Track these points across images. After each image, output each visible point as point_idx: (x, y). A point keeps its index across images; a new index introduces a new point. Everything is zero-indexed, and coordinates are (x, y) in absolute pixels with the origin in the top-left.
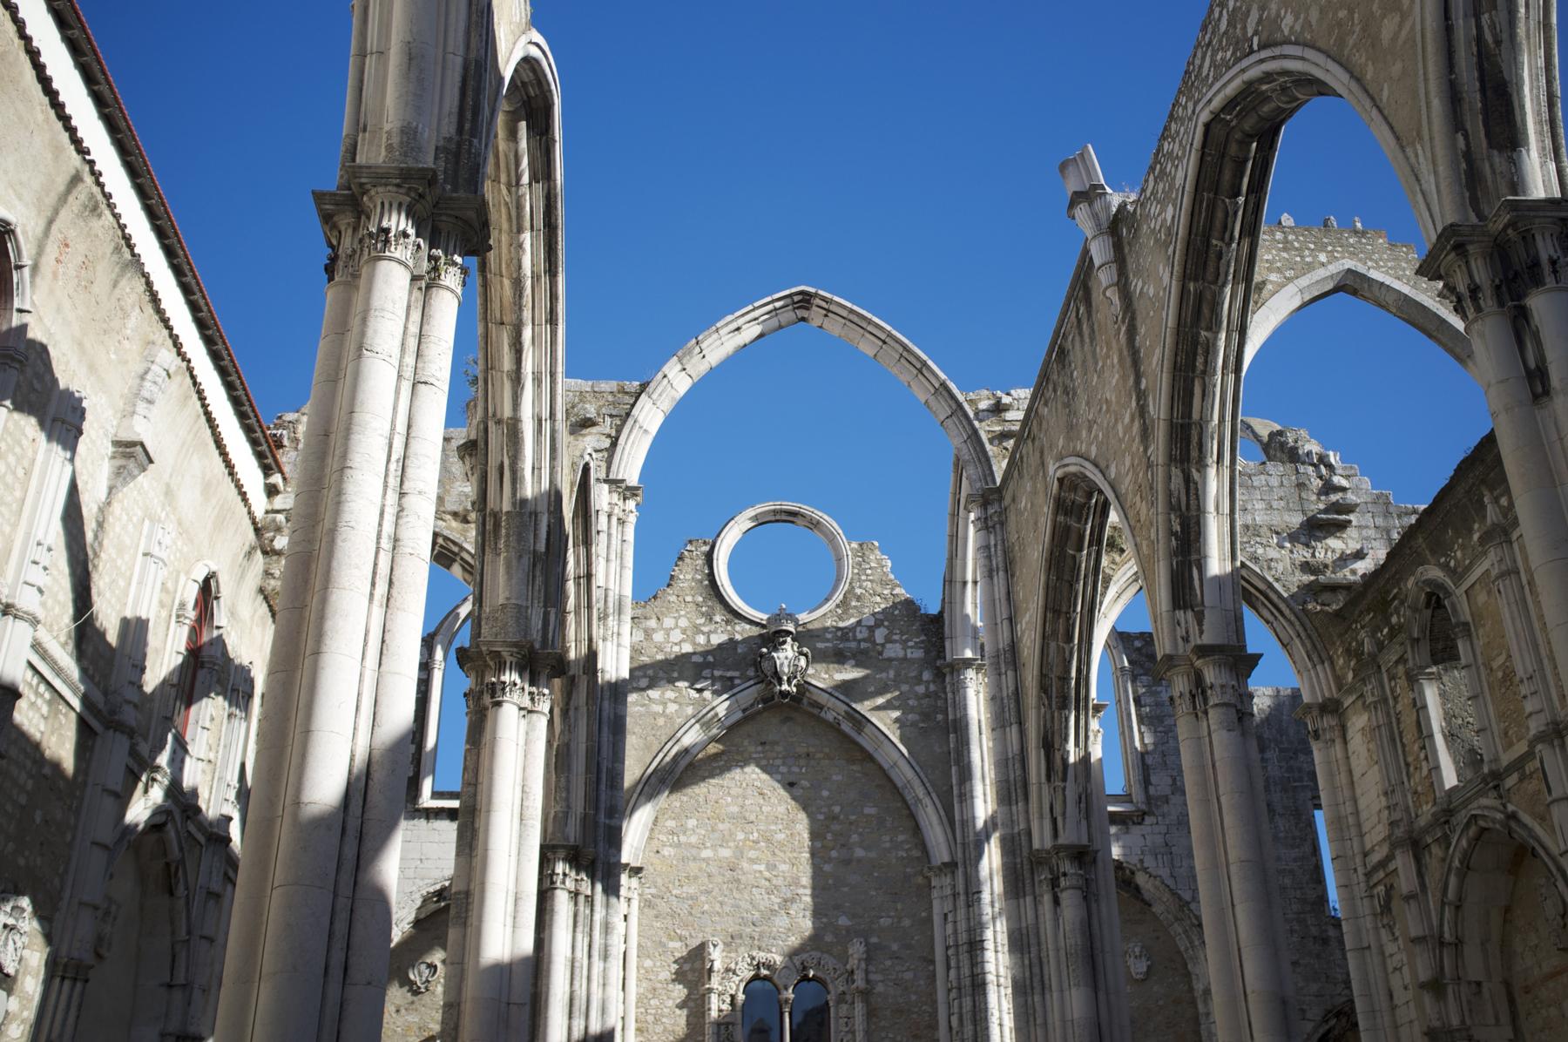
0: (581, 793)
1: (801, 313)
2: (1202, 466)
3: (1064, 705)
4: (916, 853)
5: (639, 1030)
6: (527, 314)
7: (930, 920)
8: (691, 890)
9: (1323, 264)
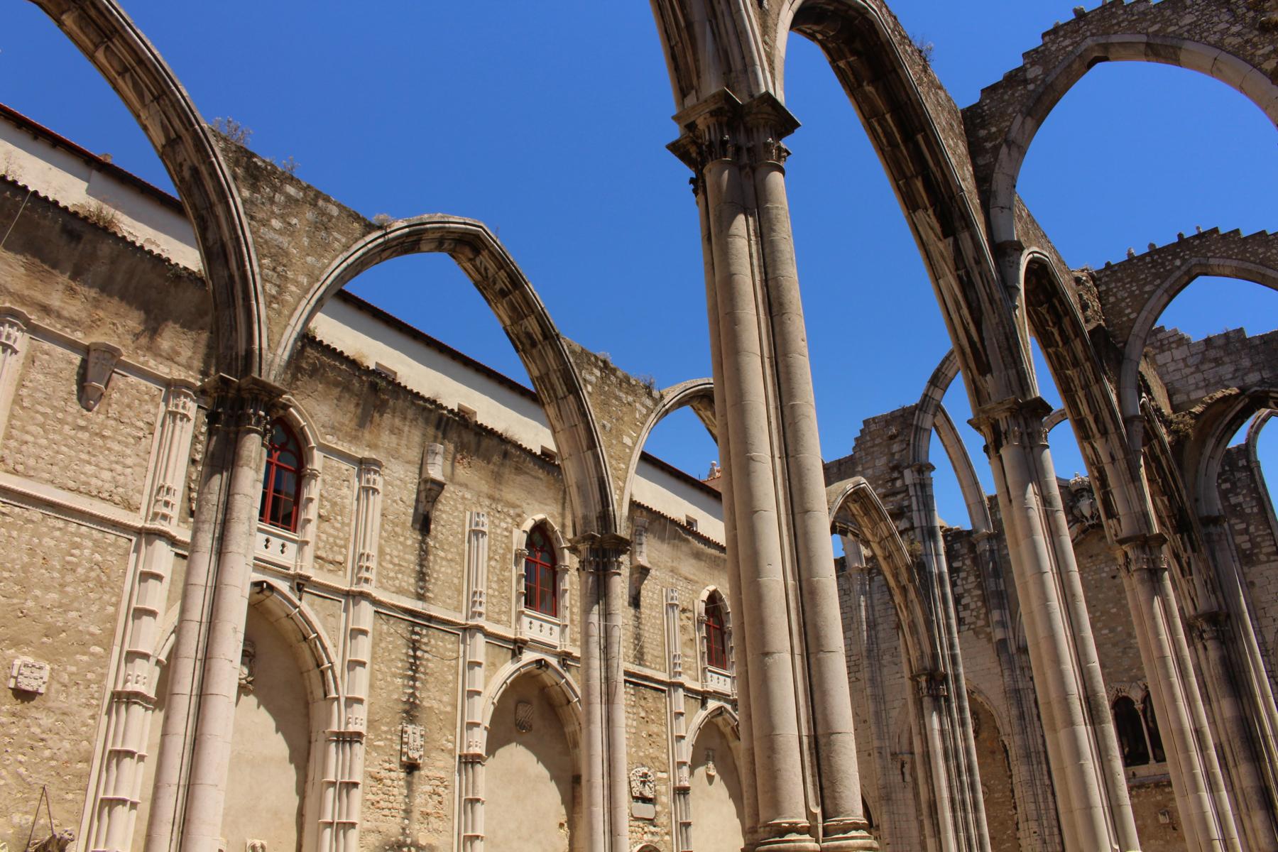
9: (1179, 268)
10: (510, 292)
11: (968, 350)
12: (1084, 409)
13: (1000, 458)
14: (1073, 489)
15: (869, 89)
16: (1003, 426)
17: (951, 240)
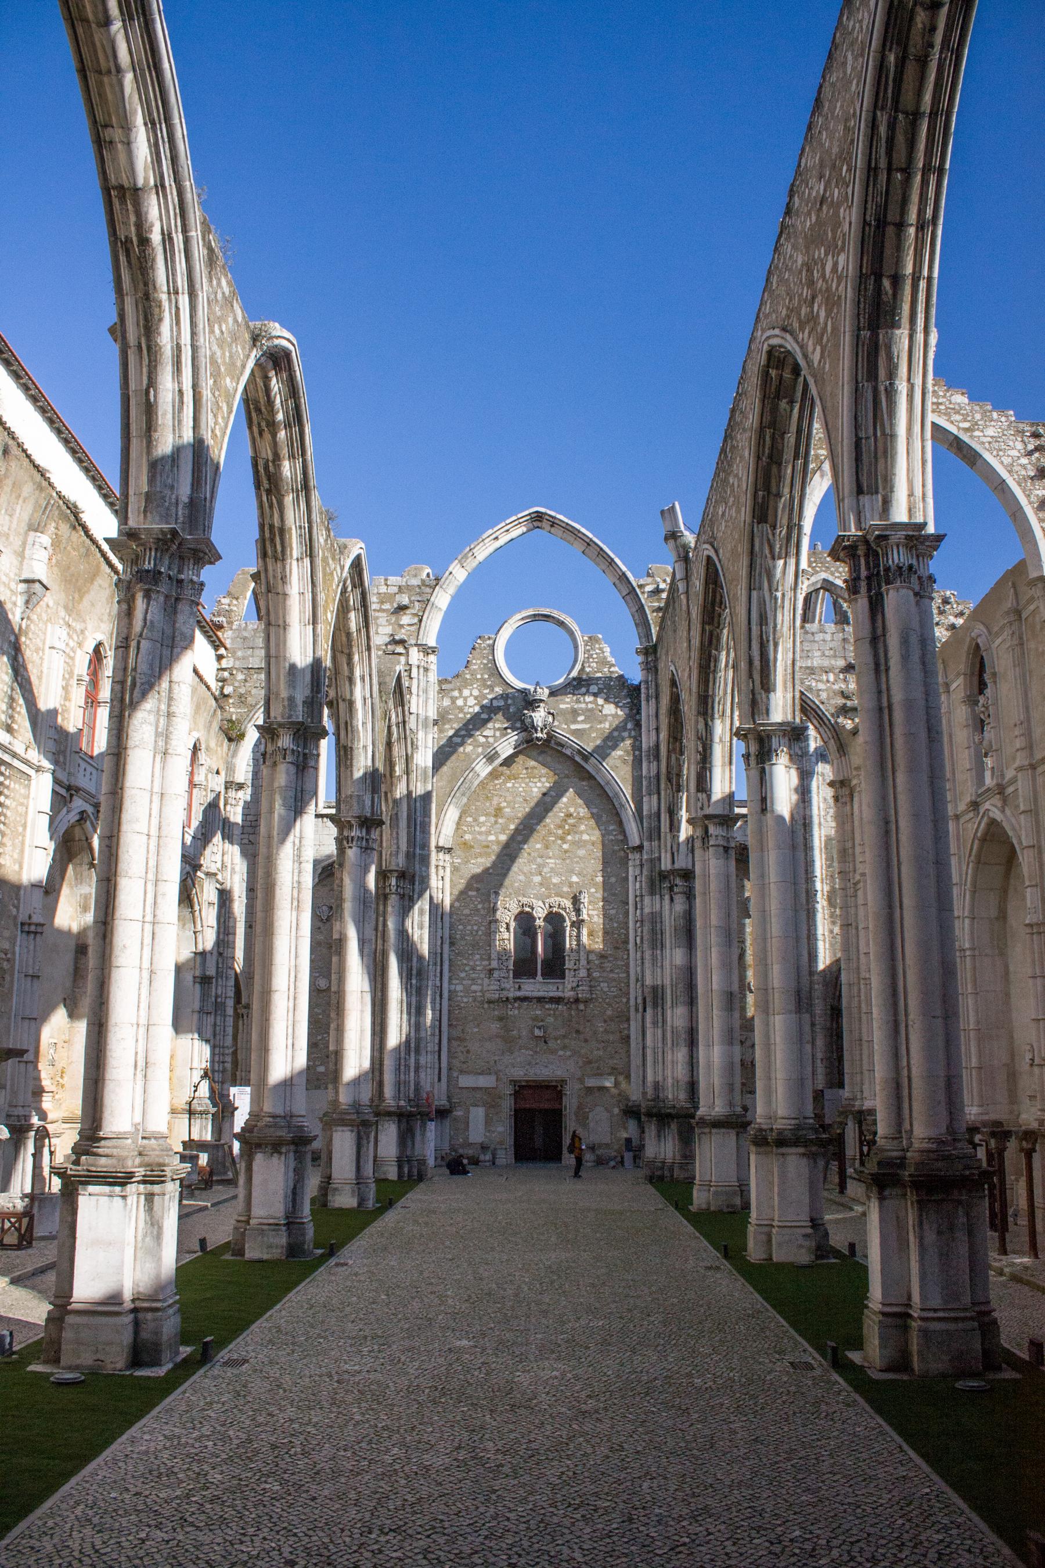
0: (405, 840)
1: (536, 524)
2: (713, 719)
3: (679, 791)
4: (621, 837)
5: (452, 944)
6: (355, 649)
7: (626, 879)
11: (757, 663)
17: (781, 562)
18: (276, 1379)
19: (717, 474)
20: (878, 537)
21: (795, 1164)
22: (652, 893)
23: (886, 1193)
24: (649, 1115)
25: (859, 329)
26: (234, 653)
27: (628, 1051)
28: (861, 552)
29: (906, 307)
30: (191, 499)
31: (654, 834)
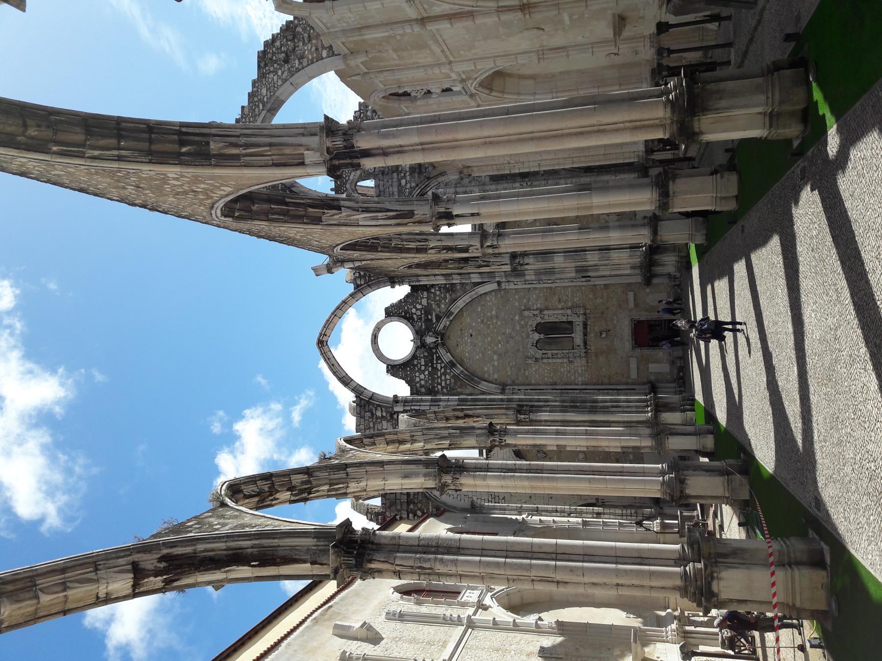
5: (555, 384)
8: (508, 368)
10: (273, 484)
12: (413, 245)
13: (457, 216)
14: (419, 344)
15: (255, 207)
16: (442, 210)
18: (827, 479)
19: (296, 246)
20: (328, 153)
21: (678, 186)
22: (524, 275)
23: (697, 130)
24: (650, 271)
25: (210, 165)
26: (398, 511)
27: (613, 285)
28: (336, 162)
29: (197, 138)
30: (315, 537)
31: (491, 274)
